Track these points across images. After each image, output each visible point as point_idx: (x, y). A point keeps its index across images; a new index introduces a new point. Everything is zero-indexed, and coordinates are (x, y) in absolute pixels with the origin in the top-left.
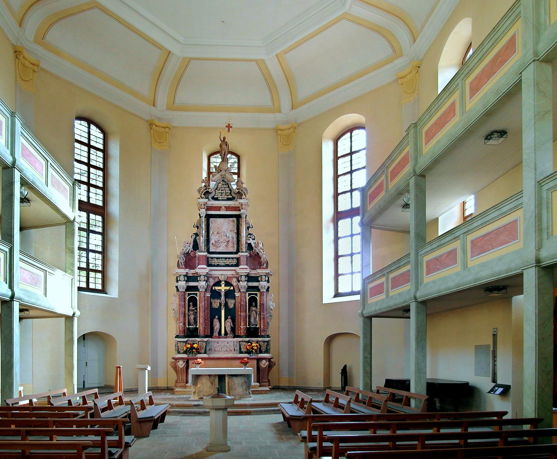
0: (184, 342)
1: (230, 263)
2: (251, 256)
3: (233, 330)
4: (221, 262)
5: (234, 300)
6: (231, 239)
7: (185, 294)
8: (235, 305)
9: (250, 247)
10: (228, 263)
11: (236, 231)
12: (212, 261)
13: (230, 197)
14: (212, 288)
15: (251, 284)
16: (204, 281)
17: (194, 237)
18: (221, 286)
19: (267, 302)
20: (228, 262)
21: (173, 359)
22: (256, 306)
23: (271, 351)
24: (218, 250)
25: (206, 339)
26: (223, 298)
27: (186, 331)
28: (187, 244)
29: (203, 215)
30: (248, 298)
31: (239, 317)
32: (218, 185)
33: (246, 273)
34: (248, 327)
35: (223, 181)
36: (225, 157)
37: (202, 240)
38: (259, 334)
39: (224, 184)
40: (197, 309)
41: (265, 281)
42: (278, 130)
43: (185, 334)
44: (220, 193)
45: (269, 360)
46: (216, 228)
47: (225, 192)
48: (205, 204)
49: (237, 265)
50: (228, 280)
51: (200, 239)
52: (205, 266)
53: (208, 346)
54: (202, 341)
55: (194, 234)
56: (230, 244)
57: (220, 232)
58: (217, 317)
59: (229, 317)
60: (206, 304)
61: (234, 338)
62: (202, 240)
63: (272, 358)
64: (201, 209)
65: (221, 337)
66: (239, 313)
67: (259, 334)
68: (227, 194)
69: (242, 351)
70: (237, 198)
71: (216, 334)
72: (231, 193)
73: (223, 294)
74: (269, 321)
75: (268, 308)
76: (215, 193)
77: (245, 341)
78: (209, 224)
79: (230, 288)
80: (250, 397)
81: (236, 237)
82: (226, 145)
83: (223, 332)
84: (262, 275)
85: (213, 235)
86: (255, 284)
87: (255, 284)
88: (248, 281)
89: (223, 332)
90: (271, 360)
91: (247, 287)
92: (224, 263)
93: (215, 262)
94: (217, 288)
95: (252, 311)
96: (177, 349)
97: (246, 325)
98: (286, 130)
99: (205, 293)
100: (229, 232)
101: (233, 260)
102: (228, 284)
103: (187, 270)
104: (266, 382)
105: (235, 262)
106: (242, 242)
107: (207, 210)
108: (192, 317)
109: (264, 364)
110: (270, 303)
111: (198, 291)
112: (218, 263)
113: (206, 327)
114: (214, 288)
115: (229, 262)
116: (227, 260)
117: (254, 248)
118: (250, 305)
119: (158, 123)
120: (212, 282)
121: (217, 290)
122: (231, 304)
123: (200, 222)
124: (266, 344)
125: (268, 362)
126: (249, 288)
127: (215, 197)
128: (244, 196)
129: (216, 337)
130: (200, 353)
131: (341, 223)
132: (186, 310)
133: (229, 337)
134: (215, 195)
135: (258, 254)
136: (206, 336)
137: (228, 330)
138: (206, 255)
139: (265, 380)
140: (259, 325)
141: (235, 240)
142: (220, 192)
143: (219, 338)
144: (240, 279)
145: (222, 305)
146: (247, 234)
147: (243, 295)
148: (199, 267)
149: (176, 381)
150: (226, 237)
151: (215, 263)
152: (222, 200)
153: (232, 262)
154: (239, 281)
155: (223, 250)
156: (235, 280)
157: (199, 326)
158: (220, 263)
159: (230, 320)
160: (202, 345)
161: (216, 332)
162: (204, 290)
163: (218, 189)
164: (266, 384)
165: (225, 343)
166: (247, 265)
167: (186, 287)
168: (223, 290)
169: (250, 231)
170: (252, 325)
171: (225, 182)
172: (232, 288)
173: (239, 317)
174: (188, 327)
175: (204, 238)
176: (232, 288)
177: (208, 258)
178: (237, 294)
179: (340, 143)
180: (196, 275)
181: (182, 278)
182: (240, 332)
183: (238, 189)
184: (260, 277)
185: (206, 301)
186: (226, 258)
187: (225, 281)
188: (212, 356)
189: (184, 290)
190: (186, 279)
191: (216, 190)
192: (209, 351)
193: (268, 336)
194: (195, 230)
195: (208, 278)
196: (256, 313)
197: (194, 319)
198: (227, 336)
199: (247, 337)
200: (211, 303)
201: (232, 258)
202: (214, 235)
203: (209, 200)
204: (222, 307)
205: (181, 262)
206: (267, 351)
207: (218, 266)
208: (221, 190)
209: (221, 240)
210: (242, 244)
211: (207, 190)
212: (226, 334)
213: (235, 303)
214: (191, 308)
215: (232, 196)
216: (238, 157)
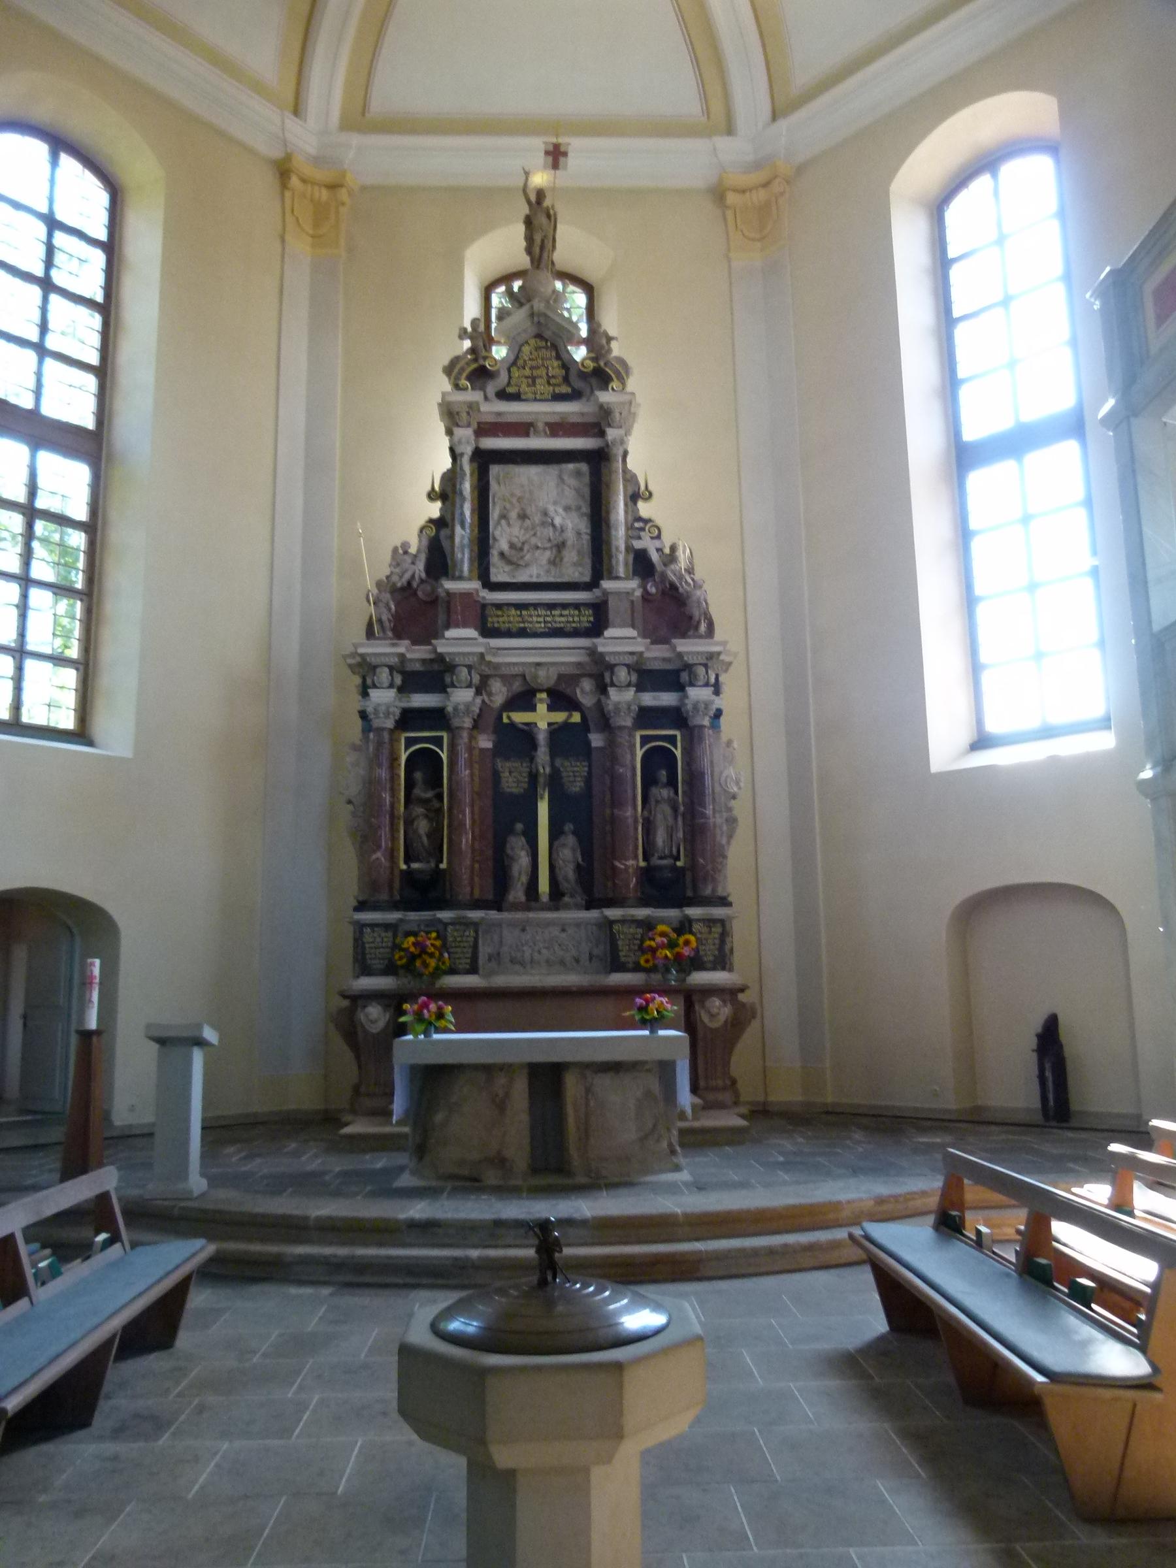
0: (387, 926)
1: (568, 622)
2: (646, 598)
3: (585, 873)
4: (536, 620)
5: (586, 763)
6: (570, 535)
7: (393, 741)
8: (588, 780)
9: (642, 564)
10: (562, 625)
11: (586, 509)
12: (498, 616)
13: (565, 389)
14: (501, 718)
15: (649, 699)
16: (469, 686)
17: (432, 532)
18: (533, 708)
19: (716, 769)
20: (560, 619)
21: (345, 997)
22: (672, 783)
23: (737, 959)
24: (523, 577)
25: (475, 915)
26: (542, 754)
27: (397, 884)
28: (406, 557)
29: (468, 450)
30: (639, 753)
31: (608, 828)
32: (520, 351)
33: (632, 653)
34: (642, 864)
35: (539, 336)
36: (545, 255)
37: (462, 535)
38: (689, 893)
39: (540, 348)
40: (440, 797)
41: (707, 685)
42: (729, 189)
43: (391, 896)
44: (527, 377)
45: (730, 994)
46: (514, 501)
47: (547, 375)
48: (472, 407)
49: (596, 629)
50: (562, 687)
51: (452, 537)
52: (471, 633)
54: (460, 924)
55: (431, 521)
56: (570, 556)
57: (528, 512)
58: (519, 826)
59: (569, 827)
60: (477, 779)
61: (588, 907)
62: (462, 535)
63: (742, 990)
64: (458, 426)
66: (608, 811)
67: (689, 893)
68: (553, 381)
69: (623, 959)
70: (588, 390)
71: (517, 893)
72: (566, 379)
73: (542, 738)
74: (724, 841)
75: (718, 789)
76: (510, 377)
78: (488, 483)
79: (570, 716)
80: (677, 1168)
81: (589, 531)
82: (549, 216)
83: (544, 886)
84: (696, 664)
85: (503, 522)
86: (667, 699)
87: (667, 699)
88: (640, 688)
89: (544, 886)
90: (741, 997)
91: (635, 708)
92: (545, 622)
93: (512, 619)
94: (519, 717)
95: (657, 802)
96: (360, 957)
97: (636, 857)
98: (754, 191)
99: (472, 738)
100: (560, 511)
101: (580, 611)
102: (560, 699)
103: (403, 647)
104: (724, 1089)
105: (586, 618)
106: (614, 543)
107: (483, 430)
108: (423, 826)
109: (717, 1012)
110: (724, 775)
111: (447, 727)
112: (522, 625)
113: (477, 866)
114: (509, 718)
115: (563, 619)
116: (557, 612)
117: (659, 567)
118: (649, 781)
119: (308, 170)
120: (499, 693)
121: (520, 726)
122: (575, 776)
123: (451, 478)
125: (729, 1005)
126: (647, 717)
127: (510, 390)
128: (615, 384)
129: (516, 907)
131: (976, 479)
132: (399, 801)
133: (567, 907)
134: (509, 384)
135: (673, 587)
136: (477, 905)
137: (568, 872)
138: (477, 591)
139: (720, 1082)
140: (686, 856)
141: (586, 538)
142: (527, 372)
143: (529, 909)
144: (608, 680)
145: (541, 780)
146: (630, 518)
147: (623, 738)
148: (449, 634)
149: (356, 1090)
150: (551, 529)
151: (510, 622)
152: (535, 400)
153: (576, 619)
154: (602, 688)
155: (538, 576)
156: (587, 685)
157: (449, 863)
158: (531, 625)
159: (571, 840)
160: (458, 939)
161: (519, 885)
162: (468, 723)
163: (520, 362)
164: (726, 1097)
166: (633, 627)
167: (398, 712)
168: (543, 725)
169: (644, 509)
170: (661, 858)
171: (546, 341)
172: (576, 718)
173: (608, 828)
174: (404, 867)
175: (468, 531)
176: (576, 718)
177: (484, 606)
178: (596, 740)
179: (952, 214)
180: (436, 667)
181: (384, 675)
182: (610, 884)
183: (592, 359)
184: (684, 670)
185: (476, 766)
186: (551, 606)
187: (551, 692)
188: (501, 981)
189: (390, 724)
190: (398, 680)
191: (514, 369)
193: (724, 902)
194: (434, 510)
195: (485, 679)
196: (675, 809)
197: (429, 836)
199: (644, 902)
200: (496, 776)
201: (577, 606)
202: (509, 525)
203: (486, 398)
204: (540, 790)
205: (380, 621)
206: (722, 962)
207: (522, 633)
208: (532, 368)
209: (534, 541)
210: (614, 550)
211: (481, 362)
212: (557, 893)
213: (590, 773)
214: (418, 792)
215: (574, 390)
216: (589, 289)
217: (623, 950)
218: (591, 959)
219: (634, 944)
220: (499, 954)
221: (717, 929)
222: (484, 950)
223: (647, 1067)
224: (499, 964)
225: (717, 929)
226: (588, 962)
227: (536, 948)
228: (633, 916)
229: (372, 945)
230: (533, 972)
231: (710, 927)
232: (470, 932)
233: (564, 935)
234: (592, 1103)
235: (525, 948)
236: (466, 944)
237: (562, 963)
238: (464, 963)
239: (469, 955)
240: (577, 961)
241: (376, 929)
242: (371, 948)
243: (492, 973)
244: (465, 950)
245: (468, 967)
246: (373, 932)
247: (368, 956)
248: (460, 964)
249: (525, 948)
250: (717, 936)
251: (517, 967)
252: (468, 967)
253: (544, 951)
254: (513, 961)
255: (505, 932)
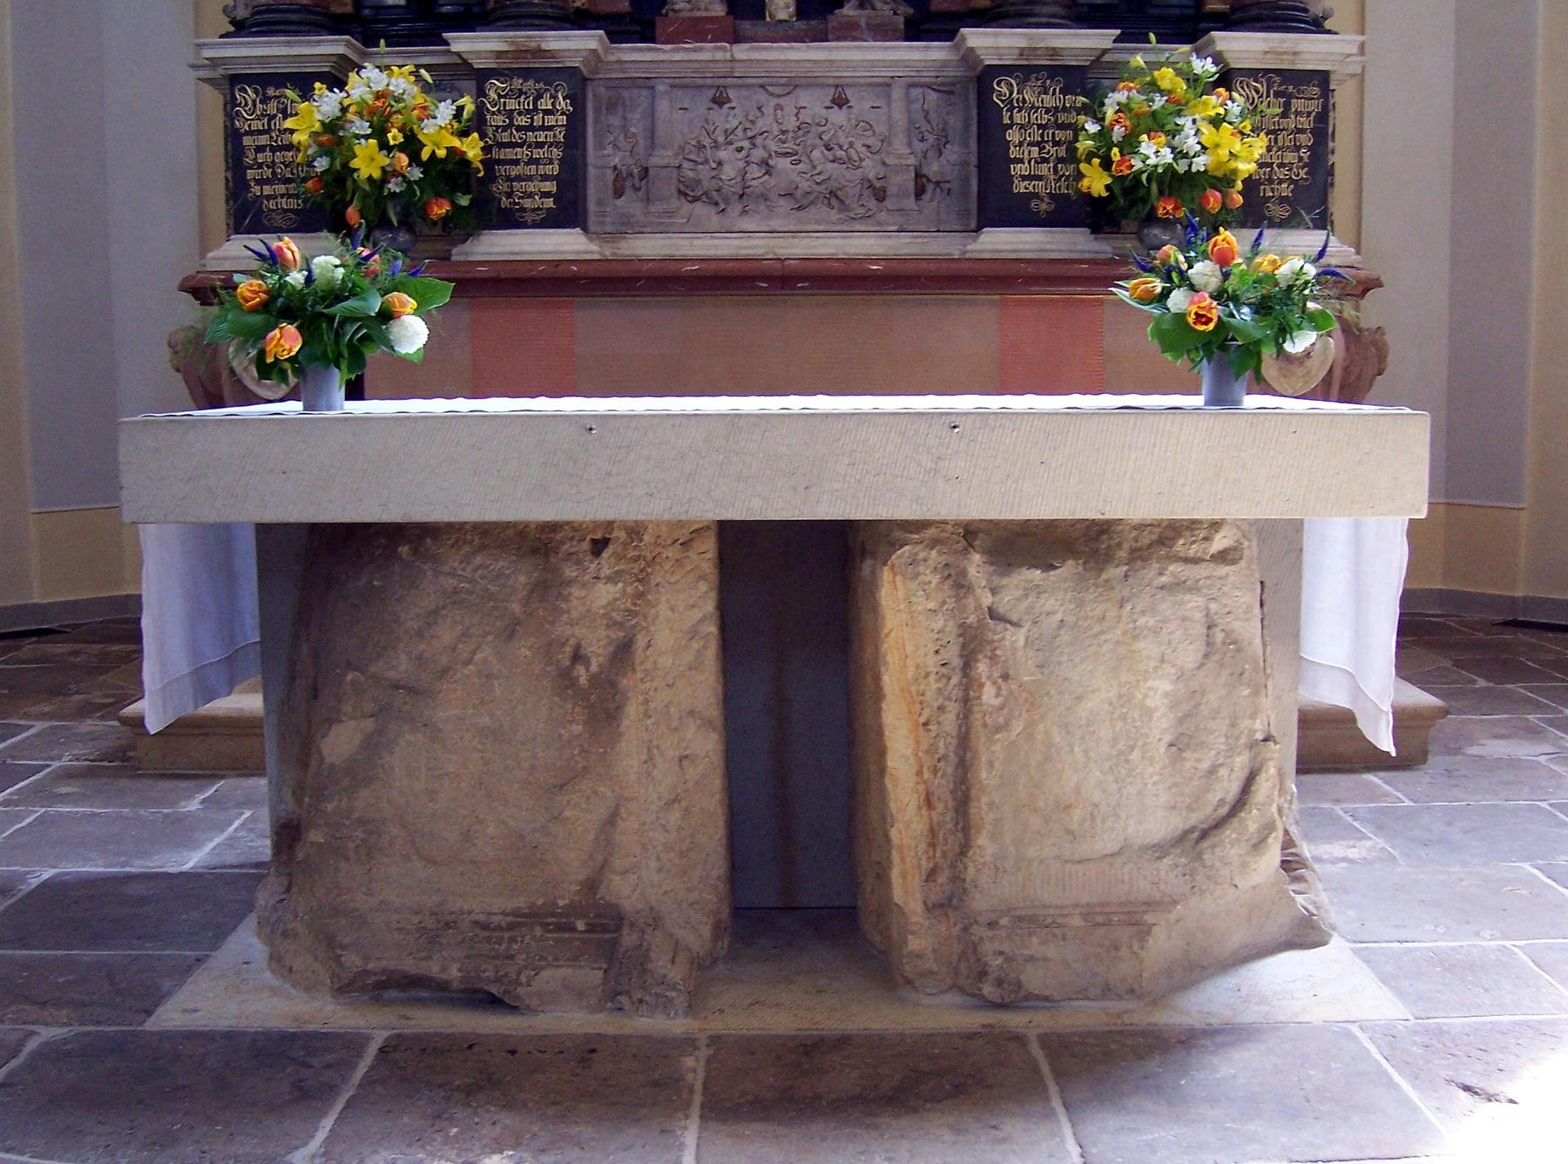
23: (1340, 202)
53: (600, 145)
54: (527, 73)
61: (915, 31)
65: (760, 30)
69: (1020, 187)
77: (1054, 71)
124: (1315, 106)
130: (511, 220)
133: (848, 32)
160: (522, 121)
165: (804, 98)
192: (618, 193)
198: (833, 22)
217: (1021, 161)
218: (919, 193)
219: (1056, 144)
220: (645, 171)
221: (1304, 105)
222: (602, 159)
223: (1219, 542)
224: (648, 200)
225: (1304, 105)
226: (912, 198)
227: (758, 154)
228: (1054, 52)
229: (263, 140)
230: (747, 224)
231: (1289, 97)
232: (554, 97)
233: (838, 116)
234: (989, 696)
235: (723, 154)
236: (542, 137)
237: (834, 197)
238: (539, 192)
239: (554, 169)
240: (880, 195)
241: (271, 92)
242: (260, 149)
243: (627, 227)
244: (538, 153)
245: (549, 203)
246: (265, 100)
247: (250, 173)
248: (531, 195)
249: (723, 154)
250: (1304, 122)
251: (701, 209)
252: (549, 203)
253: (783, 164)
254: (689, 192)
255: (663, 105)
